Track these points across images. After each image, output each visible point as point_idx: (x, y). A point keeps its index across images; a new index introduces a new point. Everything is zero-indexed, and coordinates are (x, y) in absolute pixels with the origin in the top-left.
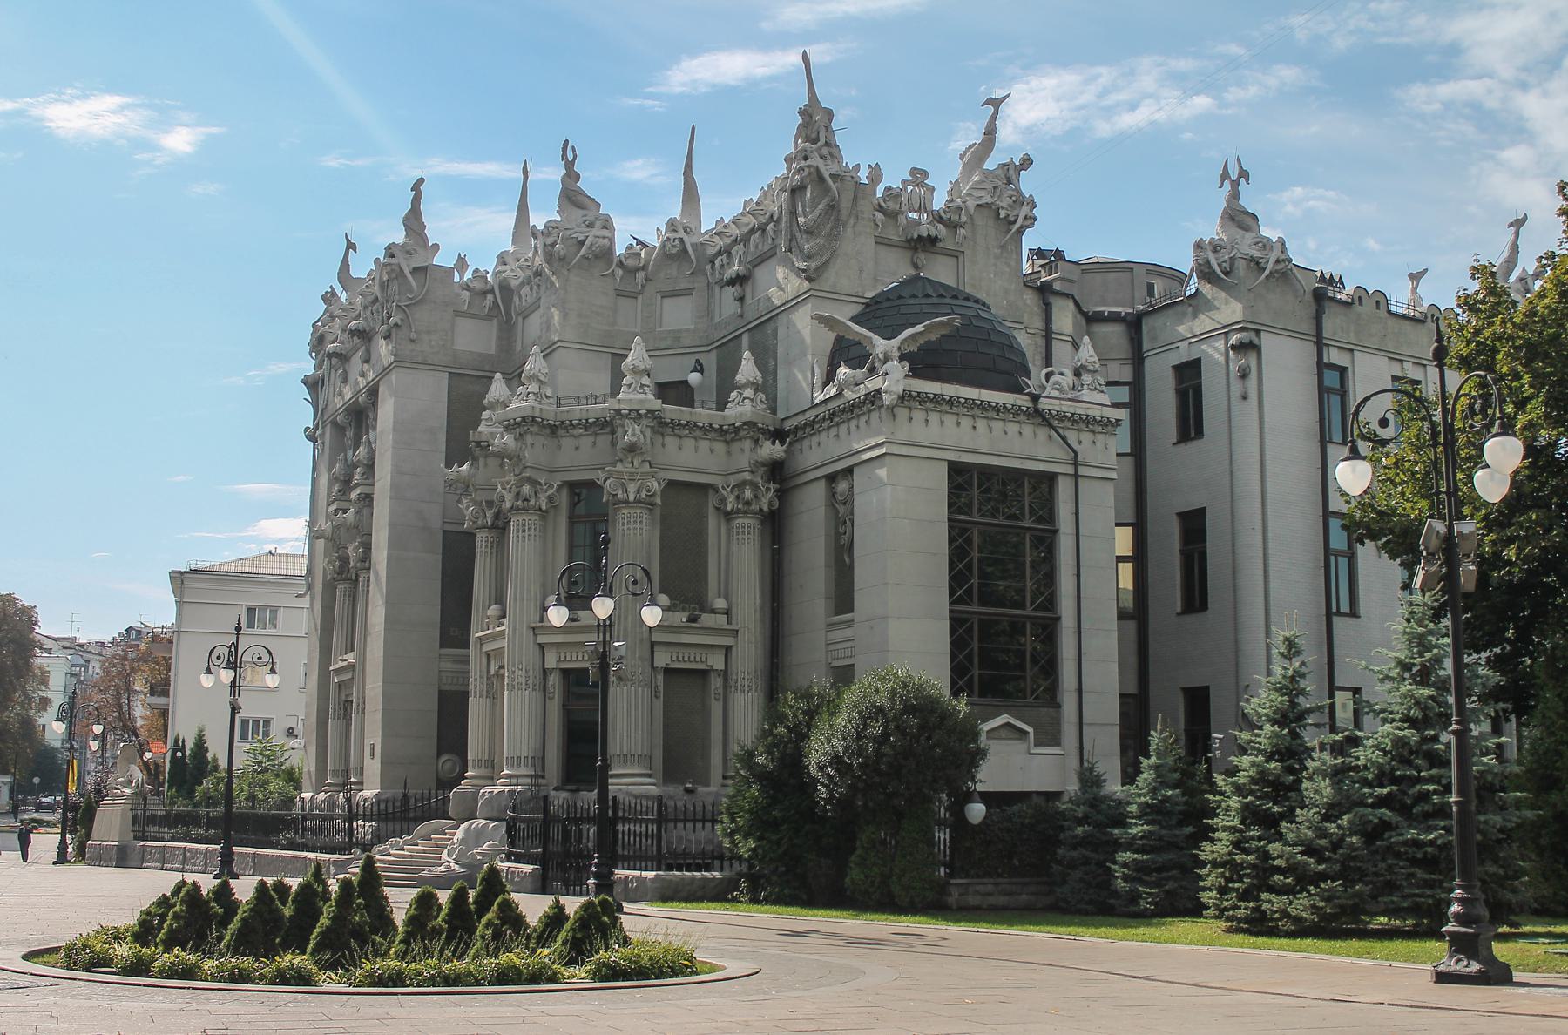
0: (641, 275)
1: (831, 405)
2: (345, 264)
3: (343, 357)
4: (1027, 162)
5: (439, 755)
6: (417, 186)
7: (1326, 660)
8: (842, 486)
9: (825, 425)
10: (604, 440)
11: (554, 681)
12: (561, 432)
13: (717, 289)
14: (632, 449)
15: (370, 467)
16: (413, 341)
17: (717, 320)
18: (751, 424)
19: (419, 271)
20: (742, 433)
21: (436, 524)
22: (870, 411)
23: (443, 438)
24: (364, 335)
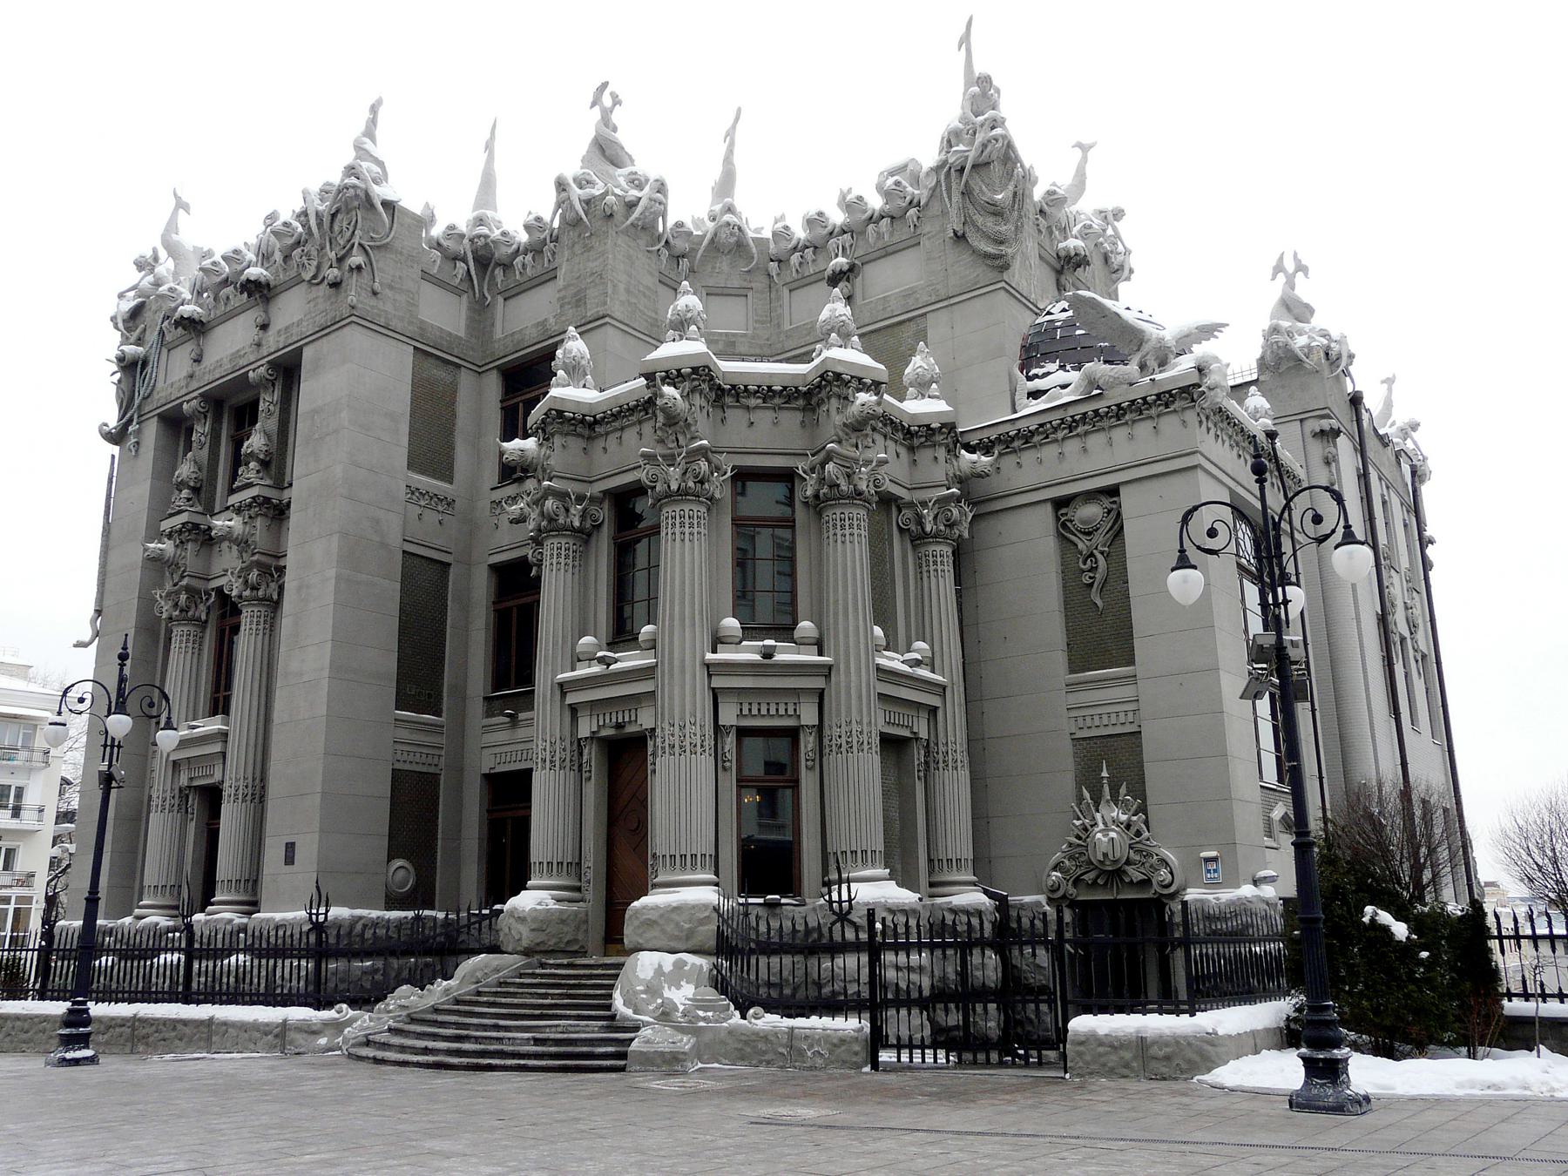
0: (685, 263)
2: (172, 226)
3: (194, 327)
4: (1118, 214)
5: (390, 859)
6: (374, 109)
7: (1399, 761)
8: (1090, 512)
9: (1060, 435)
10: (791, 419)
11: (730, 742)
12: (729, 400)
13: (786, 291)
14: (858, 426)
15: (275, 464)
16: (375, 293)
17: (787, 327)
18: (951, 427)
19: (385, 204)
20: (939, 438)
21: (395, 541)
23: (405, 428)
24: (259, 291)
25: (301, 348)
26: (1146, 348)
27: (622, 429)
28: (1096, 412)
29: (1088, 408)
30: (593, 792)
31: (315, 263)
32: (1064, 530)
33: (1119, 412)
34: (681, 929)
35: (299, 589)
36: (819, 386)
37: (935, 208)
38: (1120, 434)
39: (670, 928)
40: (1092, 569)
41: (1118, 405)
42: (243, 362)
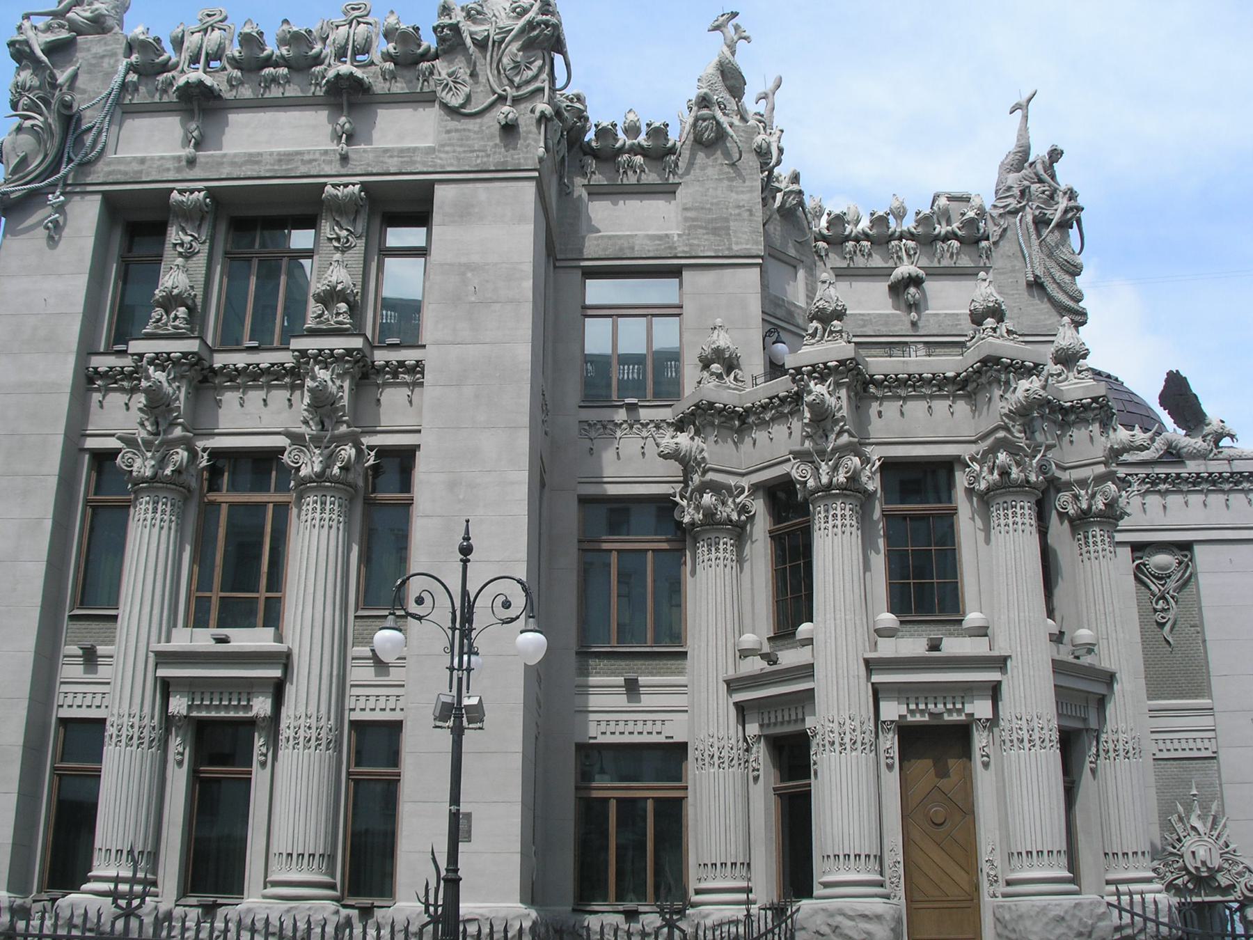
1: (1161, 471)
22: (1231, 491)
25: (432, 183)
26: (1207, 430)
27: (905, 399)
28: (1178, 475)
29: (1173, 471)
30: (892, 781)
31: (467, 90)
32: (1140, 574)
33: (1197, 480)
34: (1085, 925)
35: (452, 486)
36: (1086, 408)
37: (1006, 247)
38: (1196, 499)
39: (1075, 924)
40: (1163, 610)
41: (1198, 474)
42: (303, 170)
